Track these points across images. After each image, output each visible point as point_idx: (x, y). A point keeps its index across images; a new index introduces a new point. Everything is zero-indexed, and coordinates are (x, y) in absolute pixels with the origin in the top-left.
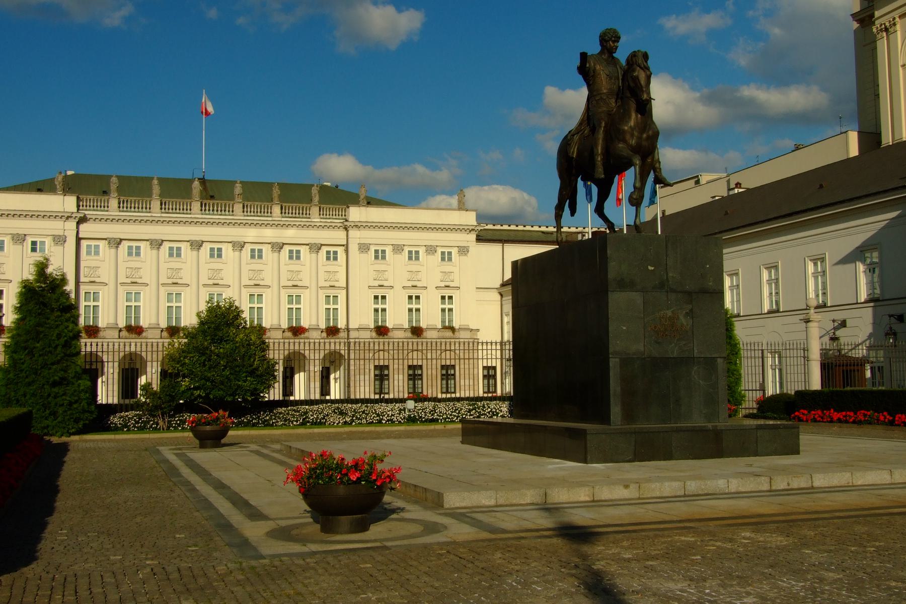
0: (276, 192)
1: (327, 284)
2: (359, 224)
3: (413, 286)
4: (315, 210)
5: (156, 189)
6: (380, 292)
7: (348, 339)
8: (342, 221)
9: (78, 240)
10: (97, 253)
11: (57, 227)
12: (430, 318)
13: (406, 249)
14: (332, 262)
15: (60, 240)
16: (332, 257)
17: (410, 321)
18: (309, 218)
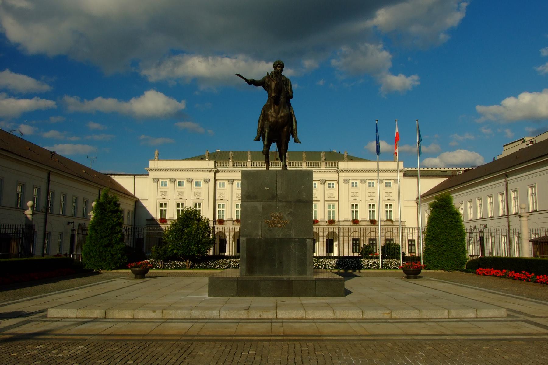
0: (304, 156)
1: (329, 199)
2: (343, 170)
3: (371, 200)
4: (323, 164)
5: (249, 157)
6: (355, 203)
7: (339, 225)
8: (335, 169)
9: (215, 181)
10: (223, 186)
11: (205, 175)
12: (380, 215)
13: (368, 182)
14: (331, 188)
15: (207, 181)
16: (331, 186)
17: (370, 217)
18: (320, 168)
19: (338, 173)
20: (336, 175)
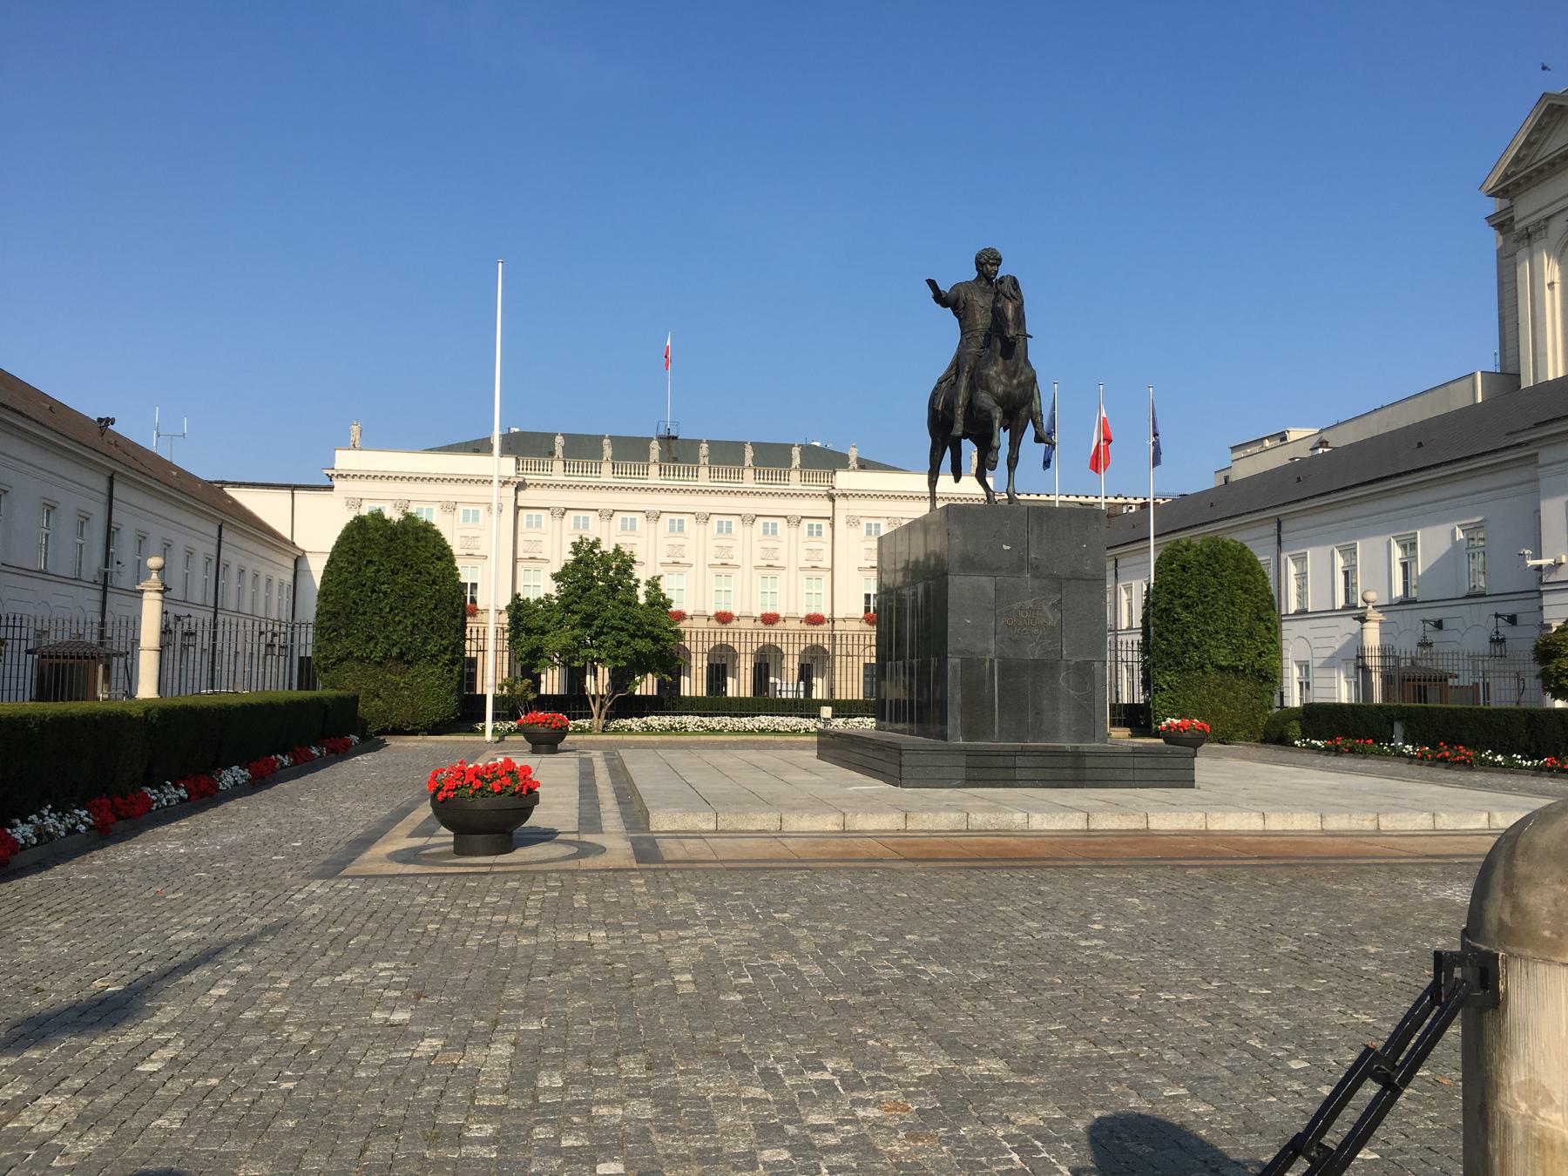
0: (749, 454)
2: (848, 493)
5: (608, 452)
9: (517, 508)
10: (539, 525)
11: (494, 493)
19: (833, 501)
20: (828, 504)
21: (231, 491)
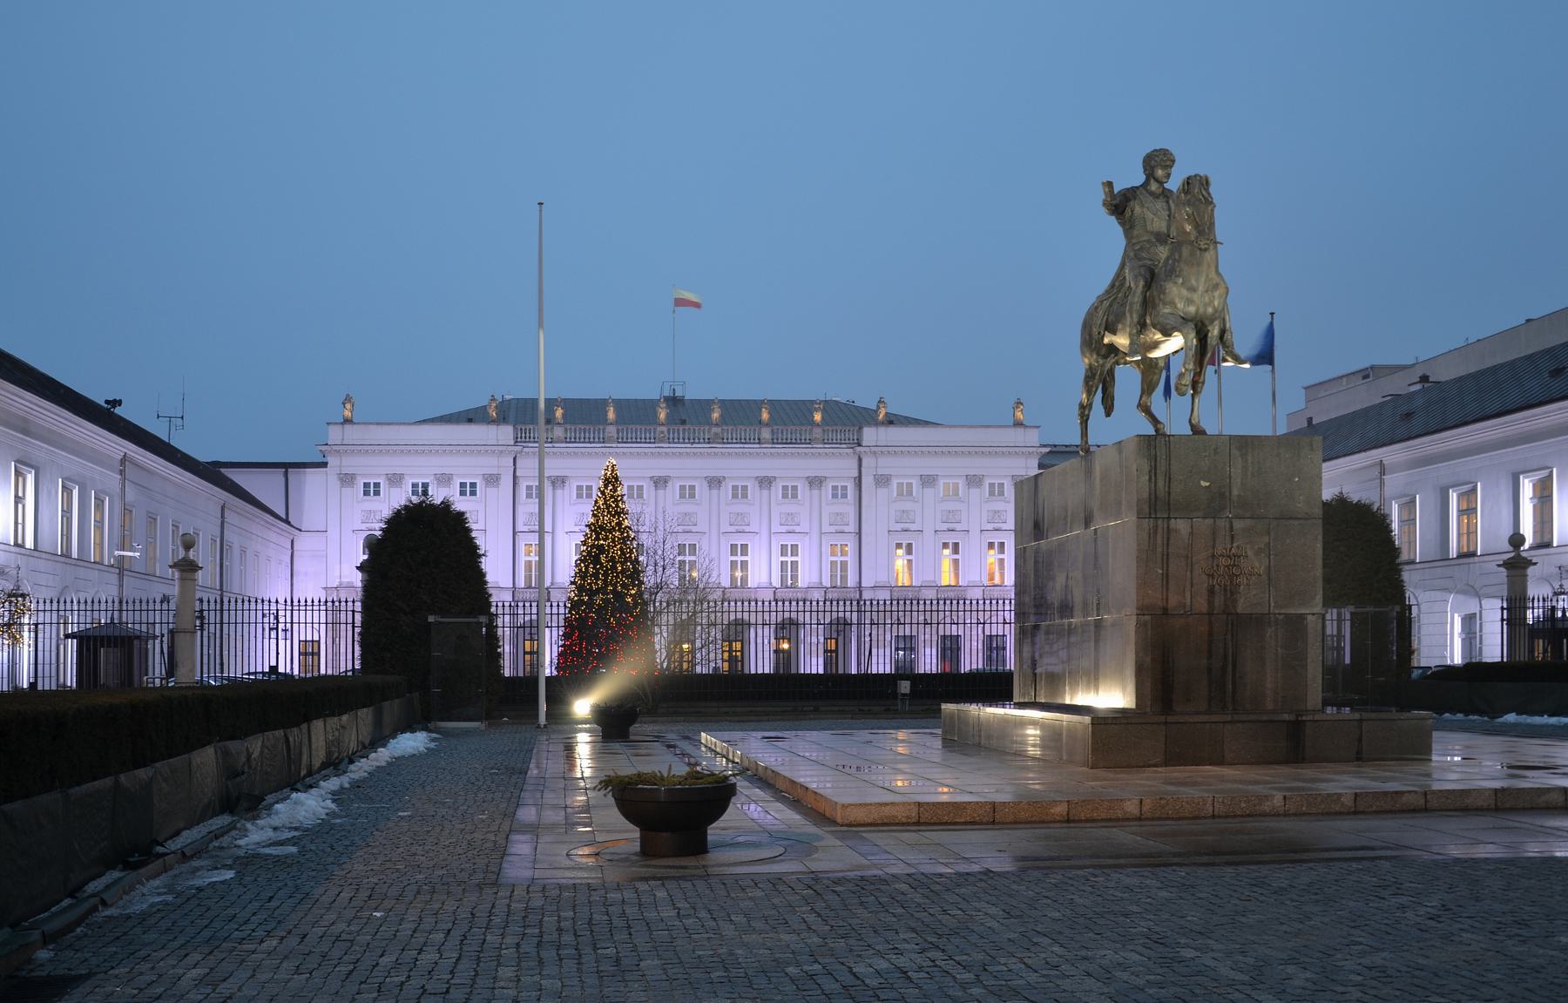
5: (611, 415)
15: (492, 480)
19: (860, 460)
21: (223, 470)
